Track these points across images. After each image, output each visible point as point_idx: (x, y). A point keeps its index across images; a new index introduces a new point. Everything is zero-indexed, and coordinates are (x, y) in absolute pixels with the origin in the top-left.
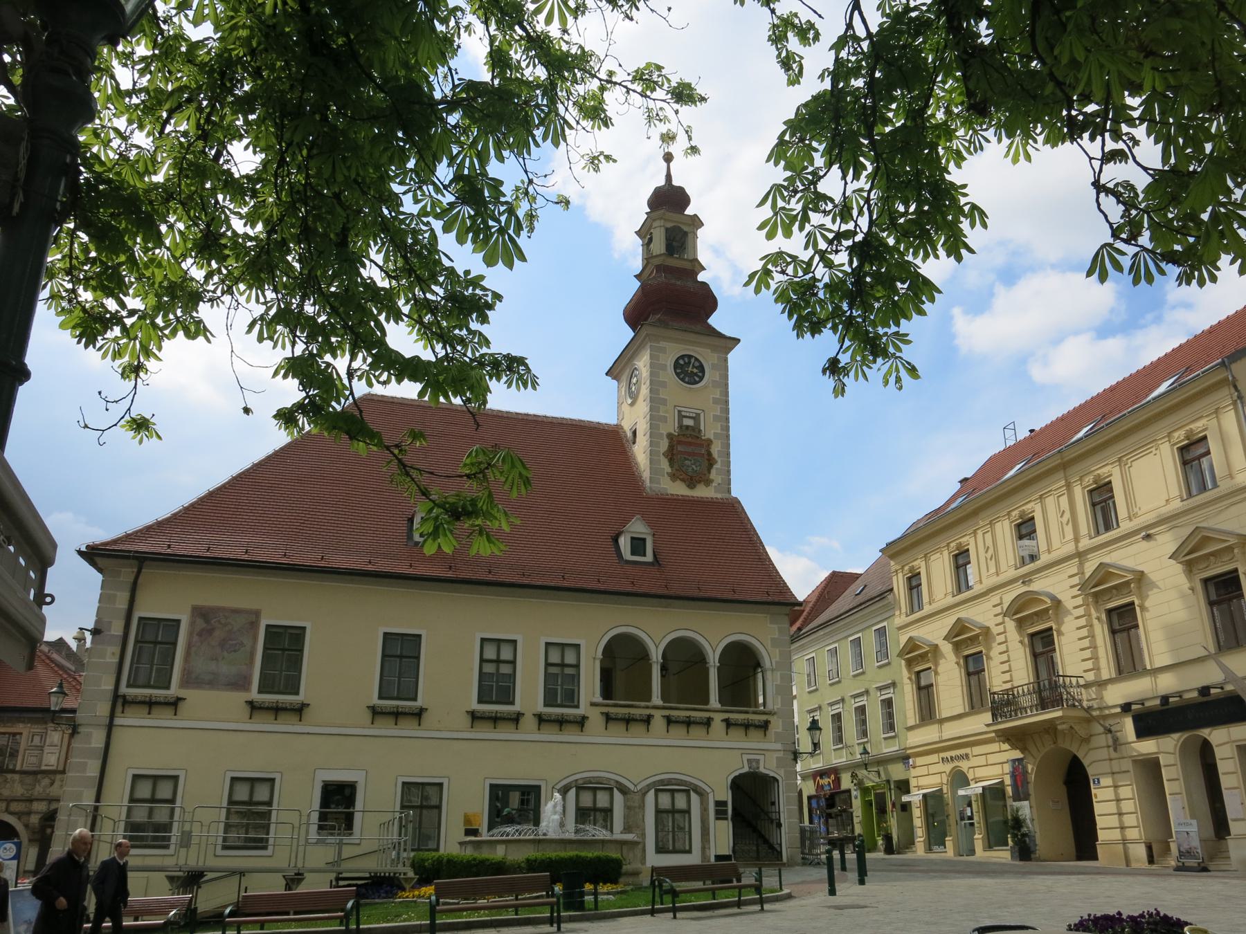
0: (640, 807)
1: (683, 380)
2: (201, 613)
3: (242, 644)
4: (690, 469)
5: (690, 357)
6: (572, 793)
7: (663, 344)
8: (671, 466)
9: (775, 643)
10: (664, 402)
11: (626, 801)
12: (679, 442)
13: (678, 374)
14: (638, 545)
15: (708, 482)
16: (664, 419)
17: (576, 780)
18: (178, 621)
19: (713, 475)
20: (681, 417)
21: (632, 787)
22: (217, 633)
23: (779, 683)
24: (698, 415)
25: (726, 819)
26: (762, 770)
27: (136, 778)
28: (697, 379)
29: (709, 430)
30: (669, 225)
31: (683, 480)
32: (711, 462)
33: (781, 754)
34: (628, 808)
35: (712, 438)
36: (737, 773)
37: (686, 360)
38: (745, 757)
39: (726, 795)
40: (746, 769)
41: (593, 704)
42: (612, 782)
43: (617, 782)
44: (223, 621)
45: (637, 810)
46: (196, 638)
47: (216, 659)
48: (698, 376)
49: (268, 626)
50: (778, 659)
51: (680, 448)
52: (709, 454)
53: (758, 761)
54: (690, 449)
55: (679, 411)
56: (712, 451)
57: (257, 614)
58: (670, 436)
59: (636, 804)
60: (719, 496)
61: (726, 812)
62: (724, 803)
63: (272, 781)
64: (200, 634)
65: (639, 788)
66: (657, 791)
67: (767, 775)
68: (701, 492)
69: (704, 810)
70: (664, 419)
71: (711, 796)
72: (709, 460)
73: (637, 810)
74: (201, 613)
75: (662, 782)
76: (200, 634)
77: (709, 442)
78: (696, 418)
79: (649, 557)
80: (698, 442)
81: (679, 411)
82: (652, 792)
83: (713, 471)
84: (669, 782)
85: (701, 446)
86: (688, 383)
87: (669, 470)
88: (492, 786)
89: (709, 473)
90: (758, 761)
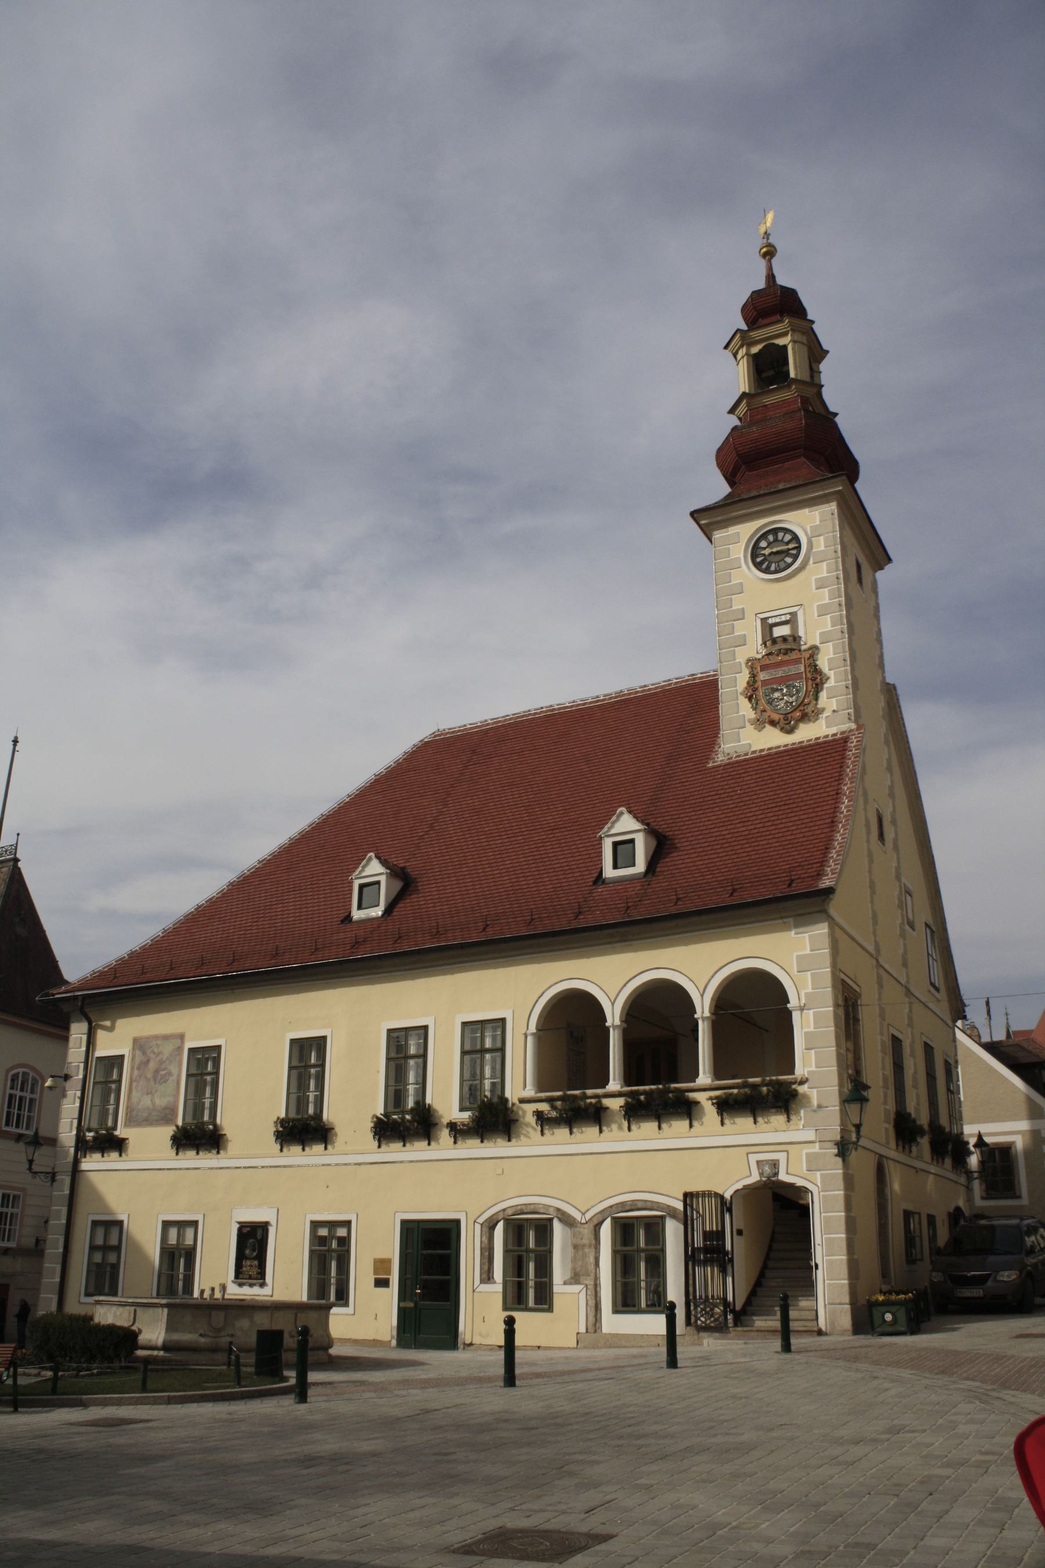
1: (767, 571)
2: (138, 1044)
3: (170, 1074)
4: (782, 704)
5: (775, 531)
6: (502, 1222)
8: (755, 709)
10: (741, 615)
12: (764, 668)
13: (758, 566)
14: (623, 850)
15: (817, 713)
16: (743, 641)
17: (504, 1210)
18: (122, 1057)
19: (825, 700)
20: (768, 627)
21: (577, 1216)
22: (152, 1065)
23: (812, 1029)
24: (794, 615)
26: (783, 1177)
27: (95, 1224)
30: (755, 350)
31: (773, 723)
33: (816, 1148)
35: (818, 643)
36: (739, 1186)
37: (771, 538)
40: (755, 1178)
41: (522, 1101)
42: (551, 1210)
43: (558, 1210)
44: (156, 1050)
45: (587, 1250)
46: (136, 1072)
47: (151, 1093)
49: (192, 1051)
50: (810, 990)
51: (762, 676)
52: (816, 666)
53: (775, 1164)
54: (780, 673)
55: (764, 621)
56: (817, 663)
57: (182, 1037)
58: (751, 663)
59: (586, 1241)
60: (834, 730)
63: (194, 1224)
64: (139, 1068)
65: (588, 1216)
66: (615, 1220)
68: (807, 733)
72: (814, 679)
73: (587, 1250)
74: (138, 1044)
76: (139, 1068)
77: (815, 649)
78: (792, 621)
83: (823, 695)
85: (797, 661)
86: (776, 572)
87: (751, 714)
88: (404, 1222)
89: (817, 699)
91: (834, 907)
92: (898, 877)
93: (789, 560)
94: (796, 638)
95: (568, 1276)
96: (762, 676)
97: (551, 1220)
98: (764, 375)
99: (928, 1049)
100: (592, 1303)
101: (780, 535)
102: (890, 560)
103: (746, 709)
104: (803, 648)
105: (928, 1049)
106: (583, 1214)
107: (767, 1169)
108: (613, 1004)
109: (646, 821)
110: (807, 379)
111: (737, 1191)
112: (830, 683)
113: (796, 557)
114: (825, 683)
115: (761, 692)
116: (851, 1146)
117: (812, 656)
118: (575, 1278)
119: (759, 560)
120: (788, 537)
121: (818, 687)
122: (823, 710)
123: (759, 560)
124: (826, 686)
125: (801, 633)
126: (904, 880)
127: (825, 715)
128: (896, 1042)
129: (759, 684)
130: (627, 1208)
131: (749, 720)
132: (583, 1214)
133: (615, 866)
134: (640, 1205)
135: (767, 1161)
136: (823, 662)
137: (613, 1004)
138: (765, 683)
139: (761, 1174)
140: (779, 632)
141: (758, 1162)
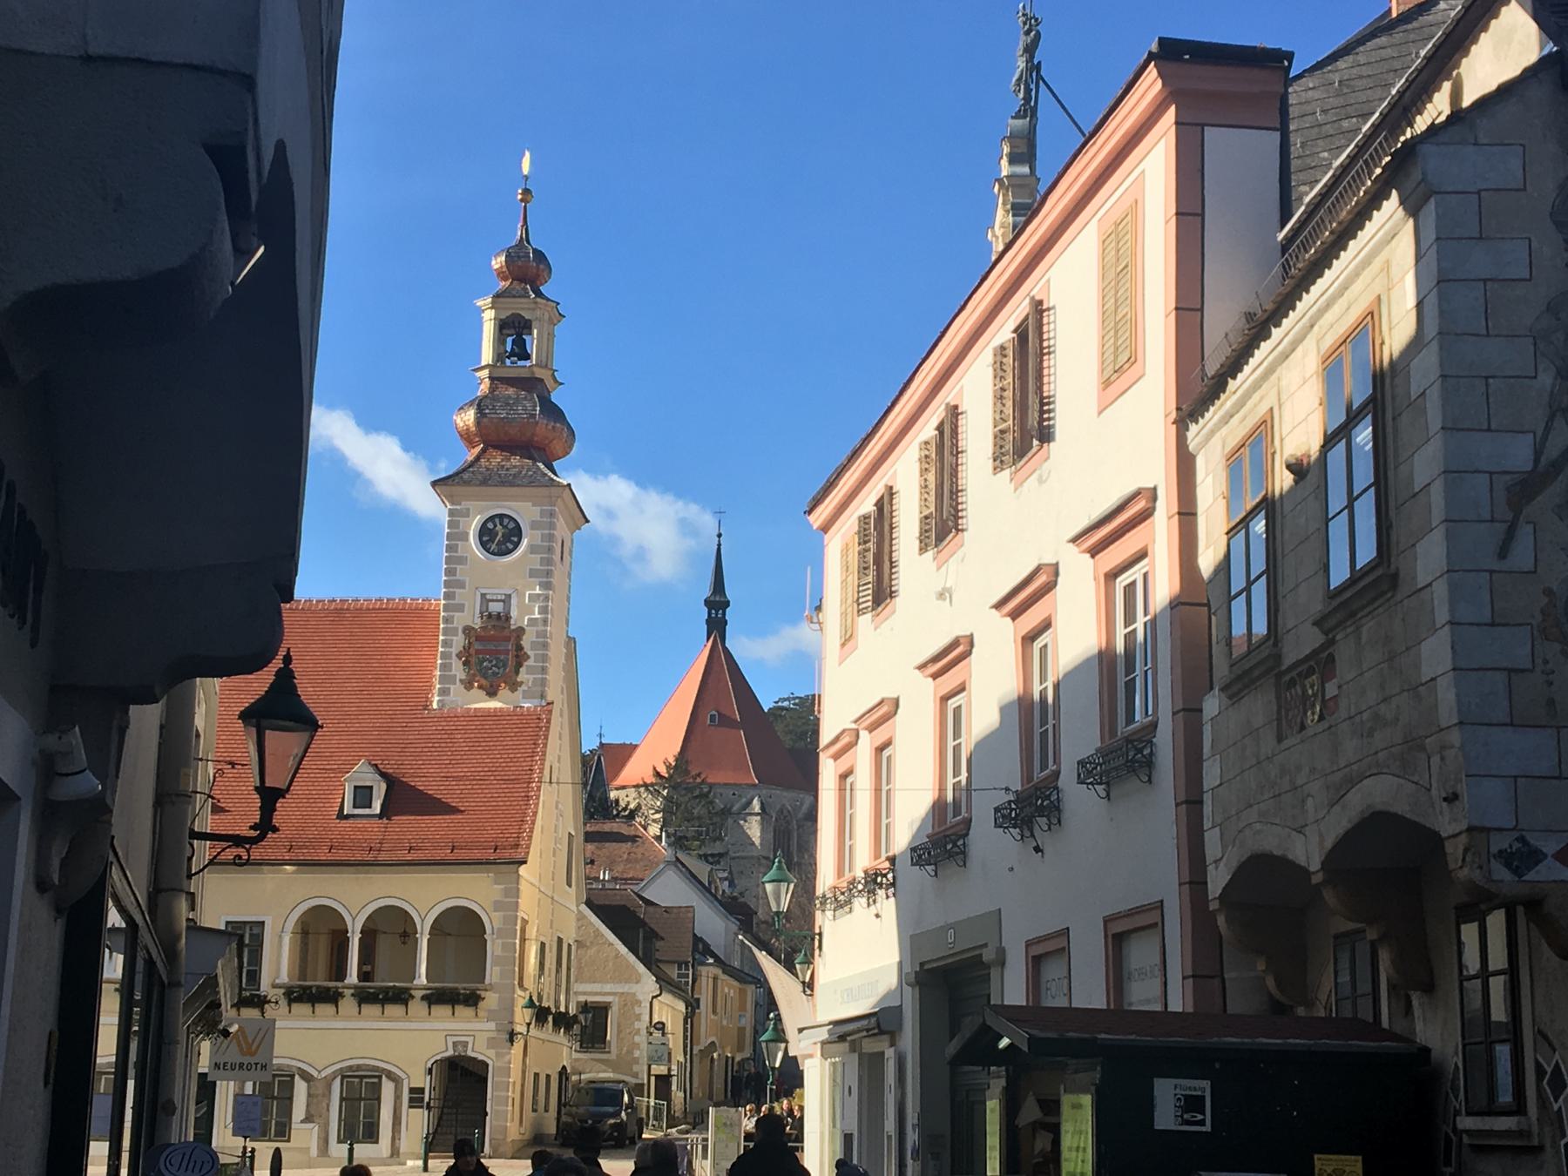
0: (324, 1095)
5: (501, 516)
7: (465, 504)
9: (498, 906)
10: (461, 585)
11: (309, 1088)
12: (478, 638)
19: (523, 676)
21: (315, 1074)
24: (509, 596)
25: (422, 1107)
26: (470, 1053)
28: (511, 546)
29: (524, 614)
32: (520, 657)
34: (309, 1095)
36: (438, 1057)
38: (451, 1040)
39: (422, 1081)
40: (450, 1053)
41: (274, 986)
42: (294, 1070)
45: (320, 1098)
48: (512, 542)
51: (477, 646)
52: (522, 648)
53: (465, 1044)
55: (483, 595)
58: (468, 630)
59: (320, 1092)
61: (423, 1098)
62: (422, 1090)
65: (323, 1074)
66: (343, 1077)
67: (475, 1059)
69: (398, 1097)
70: (460, 608)
71: (406, 1082)
72: (517, 656)
75: (350, 1068)
77: (521, 630)
78: (507, 600)
79: (377, 807)
80: (506, 633)
81: (483, 595)
82: (338, 1080)
84: (359, 1067)
85: (508, 639)
89: (517, 673)
90: (465, 1044)
91: (523, 870)
92: (557, 807)
93: (511, 546)
94: (508, 618)
95: (303, 1117)
96: (477, 646)
97: (292, 1076)
98: (505, 331)
99: (560, 940)
100: (323, 1135)
101: (506, 521)
102: (587, 521)
103: (458, 670)
104: (512, 627)
105: (560, 940)
106: (319, 1072)
107: (460, 1048)
108: (354, 919)
109: (373, 762)
110: (544, 360)
111: (436, 1062)
112: (530, 662)
113: (517, 545)
114: (526, 660)
115: (473, 660)
116: (519, 1036)
117: (519, 638)
118: (308, 1119)
119: (485, 539)
120: (512, 525)
121: (519, 665)
122: (522, 682)
123: (485, 539)
124: (526, 663)
125: (514, 613)
126: (560, 806)
127: (524, 687)
128: (543, 945)
129: (472, 651)
130: (354, 1069)
131: (461, 681)
132: (319, 1072)
133: (355, 806)
134: (364, 1068)
135: (461, 1042)
136: (526, 643)
137: (354, 919)
138: (478, 652)
139: (455, 1051)
140: (496, 608)
141: (454, 1043)
